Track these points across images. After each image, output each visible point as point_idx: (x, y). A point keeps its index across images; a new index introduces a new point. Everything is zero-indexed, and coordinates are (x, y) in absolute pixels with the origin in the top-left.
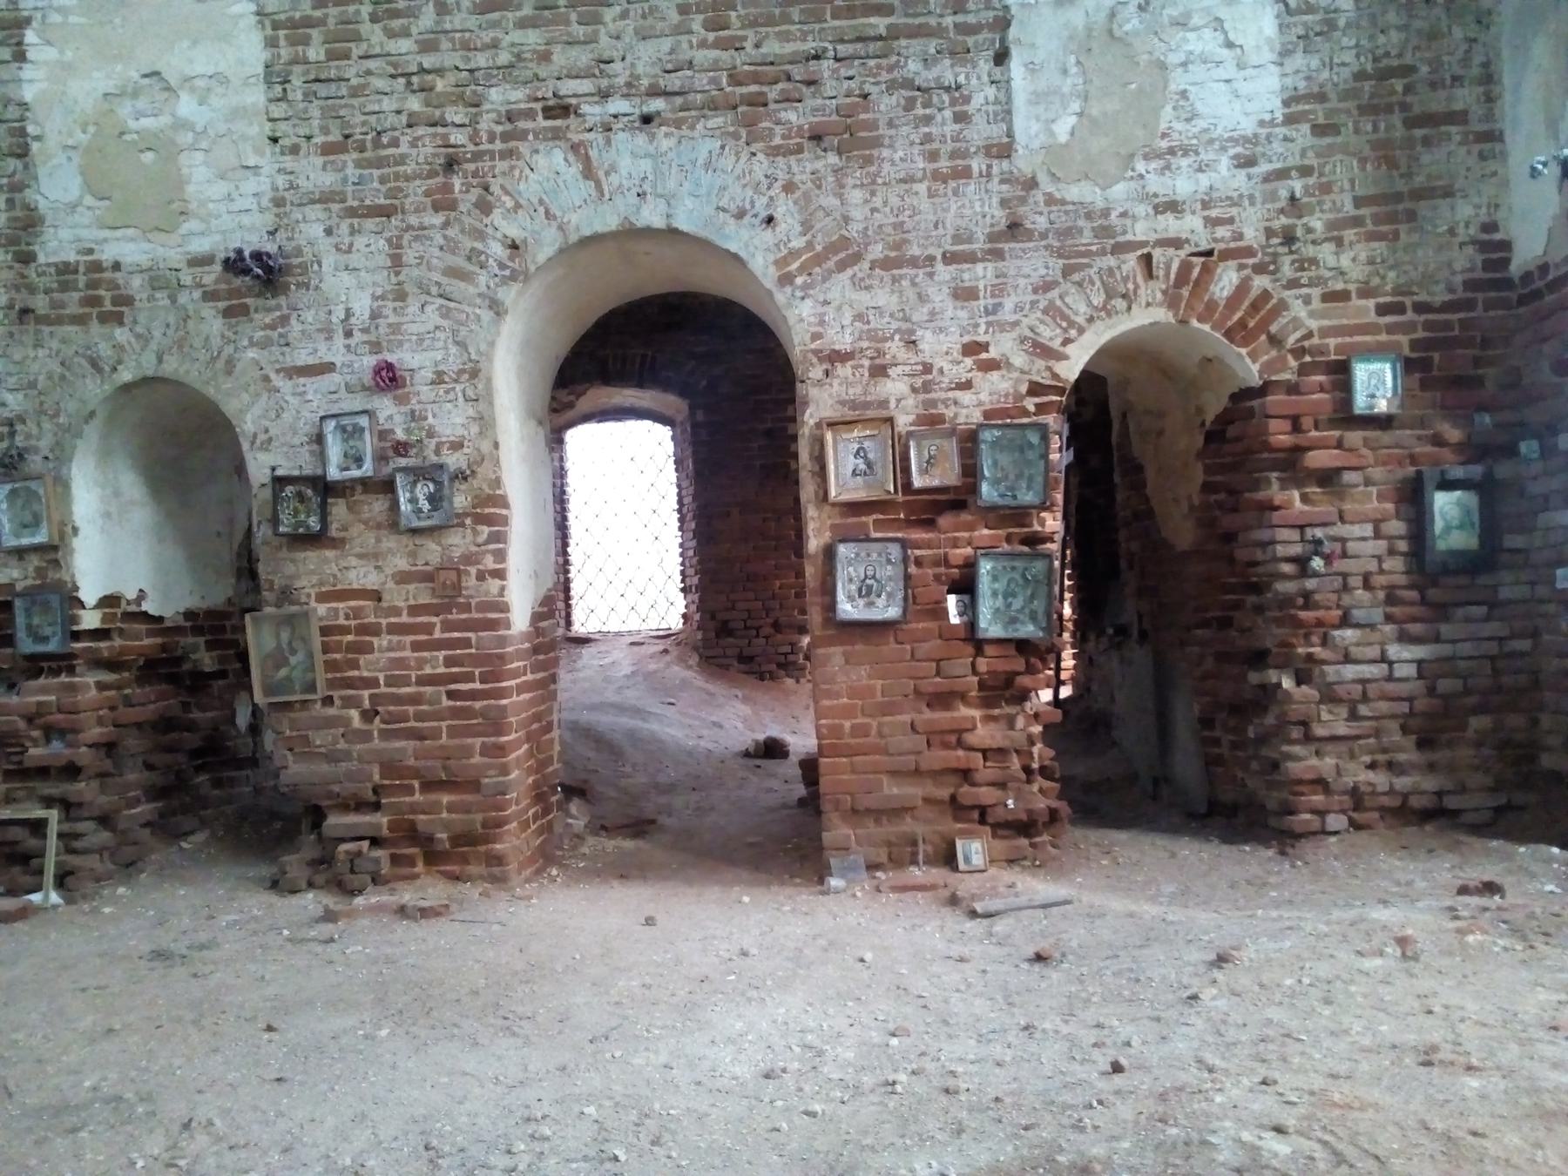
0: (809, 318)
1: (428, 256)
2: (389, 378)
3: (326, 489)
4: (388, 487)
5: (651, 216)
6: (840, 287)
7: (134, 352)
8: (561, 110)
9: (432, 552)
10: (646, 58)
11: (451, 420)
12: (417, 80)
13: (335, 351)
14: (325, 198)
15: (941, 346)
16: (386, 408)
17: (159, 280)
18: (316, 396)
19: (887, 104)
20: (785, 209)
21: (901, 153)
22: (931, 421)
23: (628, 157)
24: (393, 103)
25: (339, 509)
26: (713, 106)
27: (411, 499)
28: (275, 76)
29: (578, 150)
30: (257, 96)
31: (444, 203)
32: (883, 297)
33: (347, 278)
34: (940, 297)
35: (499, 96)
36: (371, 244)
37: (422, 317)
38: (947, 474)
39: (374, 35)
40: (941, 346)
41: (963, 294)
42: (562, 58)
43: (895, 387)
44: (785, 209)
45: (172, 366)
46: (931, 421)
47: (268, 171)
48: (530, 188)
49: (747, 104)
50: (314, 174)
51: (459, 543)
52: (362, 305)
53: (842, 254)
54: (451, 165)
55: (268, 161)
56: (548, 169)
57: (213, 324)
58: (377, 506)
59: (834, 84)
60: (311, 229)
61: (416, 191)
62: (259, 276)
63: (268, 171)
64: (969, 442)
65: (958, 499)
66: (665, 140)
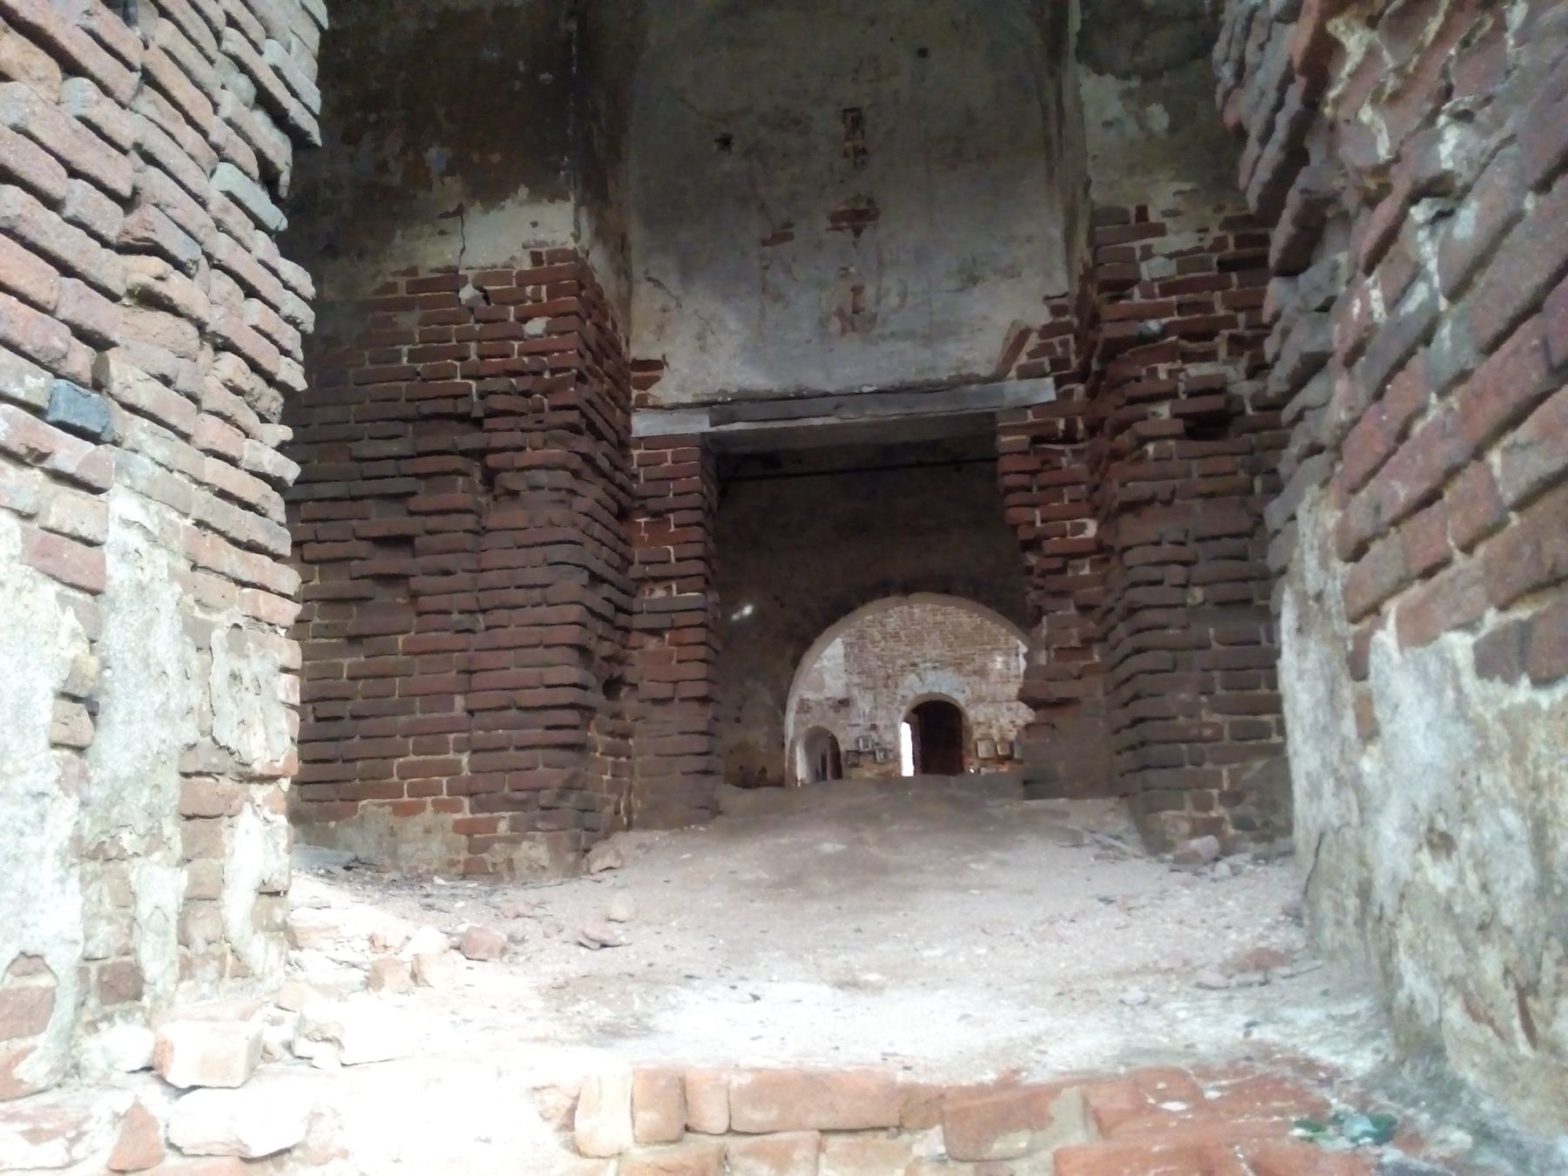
0: (974, 714)
1: (883, 699)
2: (874, 727)
3: (858, 753)
4: (873, 753)
5: (936, 690)
6: (981, 707)
7: (813, 721)
8: (914, 665)
9: (884, 769)
10: (934, 653)
11: (888, 737)
12: (880, 658)
13: (861, 721)
14: (858, 685)
15: (1004, 721)
16: (873, 734)
17: (819, 703)
18: (856, 732)
19: (990, 665)
20: (967, 689)
21: (993, 678)
22: (1003, 739)
23: (931, 677)
24: (874, 663)
25: (862, 758)
26: (950, 665)
27: (880, 756)
28: (846, 656)
29: (918, 675)
30: (842, 661)
31: (886, 686)
32: (991, 710)
33: (864, 704)
34: (1004, 710)
35: (900, 662)
36: (869, 696)
37: (882, 713)
38: (1007, 752)
39: (870, 646)
40: (1004, 721)
41: (1009, 709)
42: (915, 653)
43: (995, 732)
44: (967, 689)
45: (822, 724)
46: (1003, 739)
47: (844, 678)
48: (907, 683)
49: (958, 665)
50: (856, 679)
51: (890, 767)
52: (867, 710)
53: (981, 699)
54: (889, 677)
55: (844, 676)
56: (912, 679)
57: (831, 713)
58: (871, 757)
59: (979, 661)
60: (855, 692)
61: (880, 683)
62: (844, 703)
63: (844, 678)
64: (1011, 744)
65: (1009, 758)
66: (939, 673)
